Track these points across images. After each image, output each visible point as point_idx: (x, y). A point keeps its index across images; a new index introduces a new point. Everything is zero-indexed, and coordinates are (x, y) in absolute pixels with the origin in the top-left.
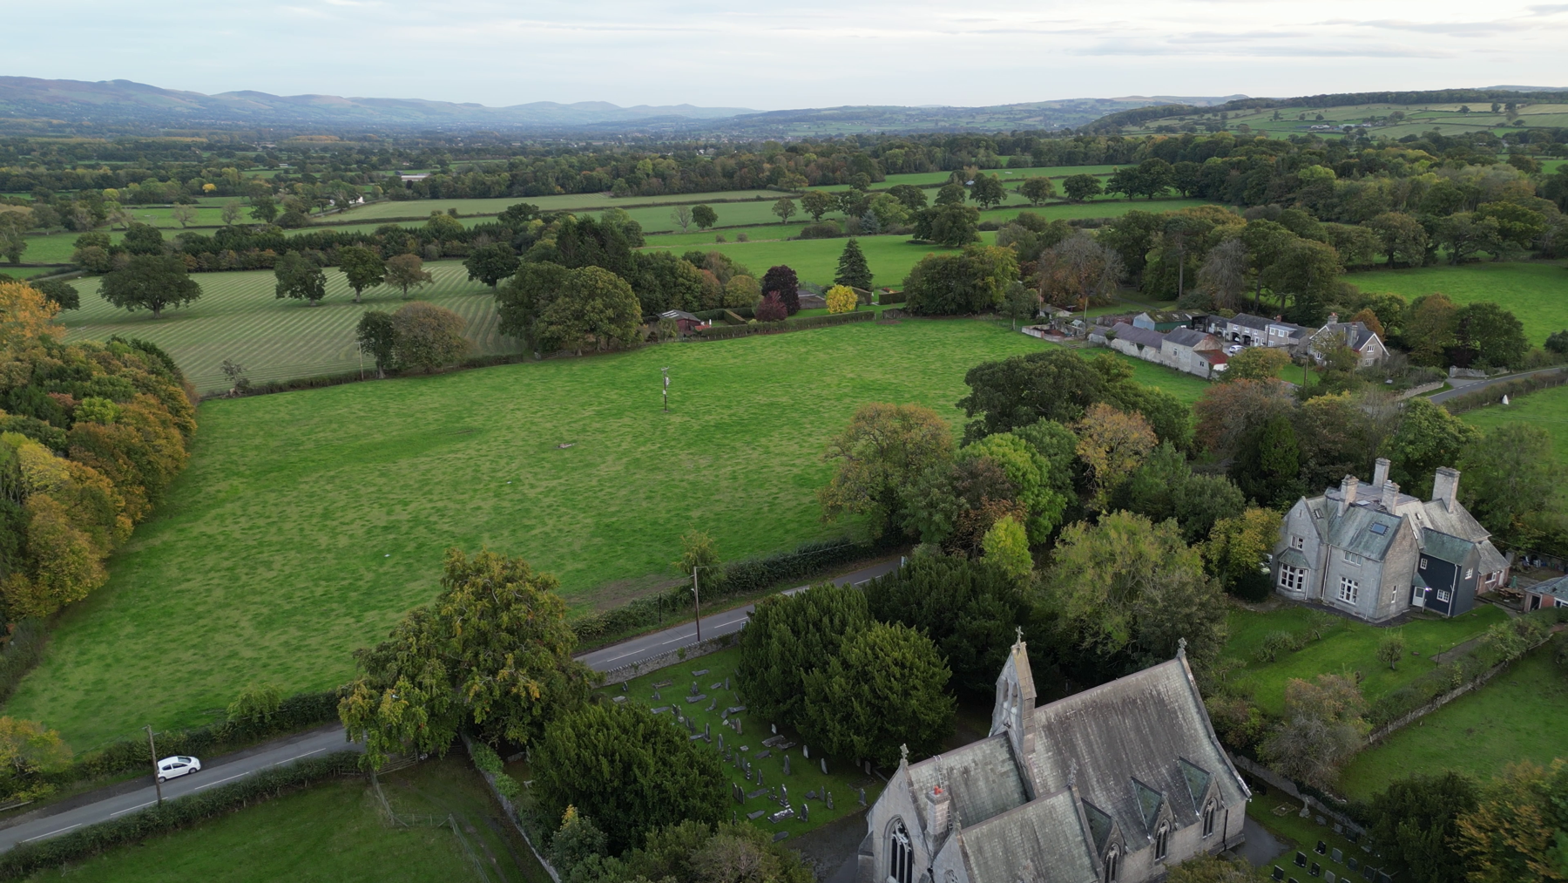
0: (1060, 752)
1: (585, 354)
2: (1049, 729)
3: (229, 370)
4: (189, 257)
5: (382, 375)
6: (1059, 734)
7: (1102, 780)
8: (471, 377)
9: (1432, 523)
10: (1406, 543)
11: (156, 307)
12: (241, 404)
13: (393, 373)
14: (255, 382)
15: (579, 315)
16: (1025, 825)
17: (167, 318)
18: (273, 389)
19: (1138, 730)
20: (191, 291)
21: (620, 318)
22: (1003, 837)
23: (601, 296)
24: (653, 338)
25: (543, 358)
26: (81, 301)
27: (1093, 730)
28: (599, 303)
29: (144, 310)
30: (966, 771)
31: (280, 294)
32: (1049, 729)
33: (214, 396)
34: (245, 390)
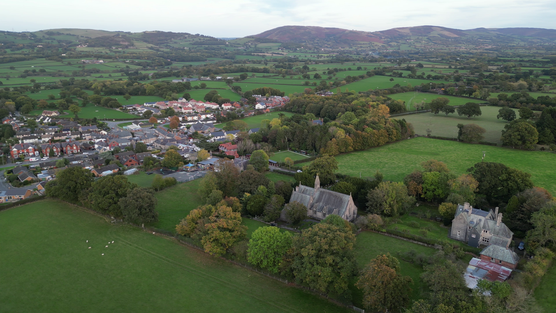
0: (320, 195)
1: (515, 148)
2: (321, 192)
3: (429, 131)
4: (520, 104)
5: (458, 140)
6: (322, 193)
7: (323, 202)
8: (481, 147)
9: (484, 224)
10: (462, 221)
11: (470, 116)
12: (429, 139)
13: (462, 141)
14: (432, 134)
15: (510, 136)
16: (302, 196)
17: (470, 119)
18: (434, 137)
19: (334, 200)
20: (479, 113)
21: (523, 140)
22: (298, 195)
23: (519, 131)
24: (543, 149)
25: (502, 146)
26: (482, 113)
27: (327, 196)
28: (516, 133)
29: (467, 116)
30: (307, 190)
31: (498, 117)
32: (321, 192)
33: (424, 136)
34: (429, 136)
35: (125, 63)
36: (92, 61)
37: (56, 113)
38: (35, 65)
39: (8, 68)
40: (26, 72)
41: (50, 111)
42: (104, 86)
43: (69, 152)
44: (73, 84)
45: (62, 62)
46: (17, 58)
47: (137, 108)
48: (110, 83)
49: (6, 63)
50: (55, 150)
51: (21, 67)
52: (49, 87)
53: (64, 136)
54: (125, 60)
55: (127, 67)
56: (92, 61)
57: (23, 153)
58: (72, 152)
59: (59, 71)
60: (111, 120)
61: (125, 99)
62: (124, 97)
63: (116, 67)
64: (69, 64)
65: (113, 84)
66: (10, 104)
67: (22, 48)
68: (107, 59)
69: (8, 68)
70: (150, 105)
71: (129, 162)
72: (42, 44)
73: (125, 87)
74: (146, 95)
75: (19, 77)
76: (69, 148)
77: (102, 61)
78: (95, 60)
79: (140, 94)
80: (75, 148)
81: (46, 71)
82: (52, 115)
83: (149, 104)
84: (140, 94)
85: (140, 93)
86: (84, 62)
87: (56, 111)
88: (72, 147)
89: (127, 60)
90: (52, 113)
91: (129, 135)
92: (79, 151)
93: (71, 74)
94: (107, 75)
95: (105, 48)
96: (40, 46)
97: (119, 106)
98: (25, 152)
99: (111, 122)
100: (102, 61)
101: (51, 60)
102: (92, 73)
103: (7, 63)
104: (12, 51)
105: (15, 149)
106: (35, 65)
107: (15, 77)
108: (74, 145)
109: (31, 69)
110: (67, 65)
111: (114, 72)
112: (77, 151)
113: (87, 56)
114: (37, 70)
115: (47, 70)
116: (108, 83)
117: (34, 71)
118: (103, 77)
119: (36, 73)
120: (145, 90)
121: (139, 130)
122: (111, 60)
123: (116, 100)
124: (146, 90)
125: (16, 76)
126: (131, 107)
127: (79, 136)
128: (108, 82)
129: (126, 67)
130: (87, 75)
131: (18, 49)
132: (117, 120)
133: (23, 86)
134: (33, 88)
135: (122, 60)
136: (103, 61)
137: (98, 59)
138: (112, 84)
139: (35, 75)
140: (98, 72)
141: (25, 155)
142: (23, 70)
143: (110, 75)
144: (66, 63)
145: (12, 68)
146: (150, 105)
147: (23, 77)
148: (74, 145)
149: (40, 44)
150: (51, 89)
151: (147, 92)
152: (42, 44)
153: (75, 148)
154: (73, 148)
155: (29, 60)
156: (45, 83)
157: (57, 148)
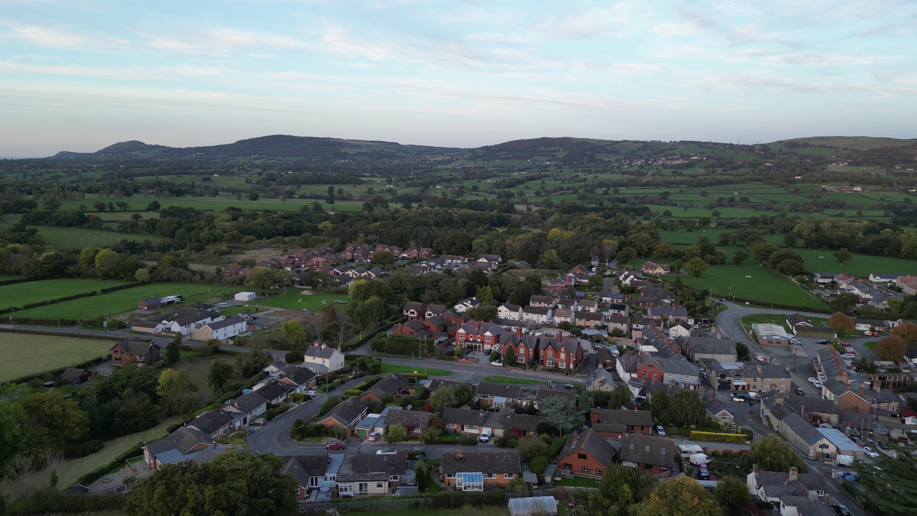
35: (907, 192)
36: (840, 188)
37: (663, 268)
38: (740, 191)
39: (699, 194)
40: (720, 199)
41: (654, 264)
42: (817, 229)
43: (549, 364)
44: (772, 223)
45: (786, 189)
46: (720, 180)
47: (840, 282)
48: (830, 225)
49: (703, 186)
50: (522, 351)
51: (715, 194)
52: (723, 225)
53: (595, 320)
54: (908, 187)
55: (907, 201)
56: (840, 188)
57: (474, 341)
58: (556, 365)
59: (772, 202)
60: (740, 301)
61: (837, 259)
62: (836, 255)
63: (882, 199)
64: (797, 191)
65: (837, 227)
66: (609, 244)
67: (740, 167)
68: (872, 184)
69: (699, 194)
70: (884, 280)
71: (576, 456)
72: (773, 161)
73: (860, 235)
74: (899, 258)
75: (705, 207)
76: (550, 353)
77: (859, 189)
78: (845, 186)
79: (886, 253)
80: (563, 356)
81: (751, 201)
82: (655, 272)
83: (882, 278)
84: (886, 253)
85: (886, 250)
86: (824, 189)
87: (665, 266)
88: (557, 352)
89: (912, 189)
90: (656, 268)
91: (728, 353)
92: (571, 366)
93: (787, 207)
94: (854, 213)
95: (879, 168)
96: (767, 164)
97: (798, 271)
98: (479, 340)
99: (738, 307)
100: (859, 189)
101: (771, 184)
102: (829, 208)
103: (705, 186)
104: (724, 170)
105: (461, 331)
106: (740, 191)
107: (698, 207)
108: (563, 349)
109: (728, 196)
110: (793, 193)
111: (874, 208)
112: (568, 365)
113: (836, 179)
114: (737, 199)
115: (752, 199)
116: (825, 225)
117: (732, 200)
118: (843, 216)
119: (732, 203)
120: (900, 245)
121: (778, 342)
122: (879, 187)
123: (798, 258)
124: (902, 244)
125: (701, 206)
126: (829, 278)
127: (624, 327)
128: (825, 223)
129: (903, 200)
130: (815, 211)
131: (734, 169)
132: (753, 303)
133: (683, 219)
134: (697, 224)
135: (902, 187)
136: (862, 188)
137: (852, 185)
138: (832, 227)
139: (732, 206)
140: (841, 206)
141: (476, 347)
142: (716, 197)
143: (860, 214)
144: (792, 189)
145: (704, 194)
146: (884, 280)
147: (711, 207)
148: (563, 349)
149: (770, 160)
150: (726, 228)
151: (903, 249)
152: (773, 161)
153: (563, 356)
154: (559, 357)
155: (737, 183)
156: (734, 219)
157: (527, 348)
